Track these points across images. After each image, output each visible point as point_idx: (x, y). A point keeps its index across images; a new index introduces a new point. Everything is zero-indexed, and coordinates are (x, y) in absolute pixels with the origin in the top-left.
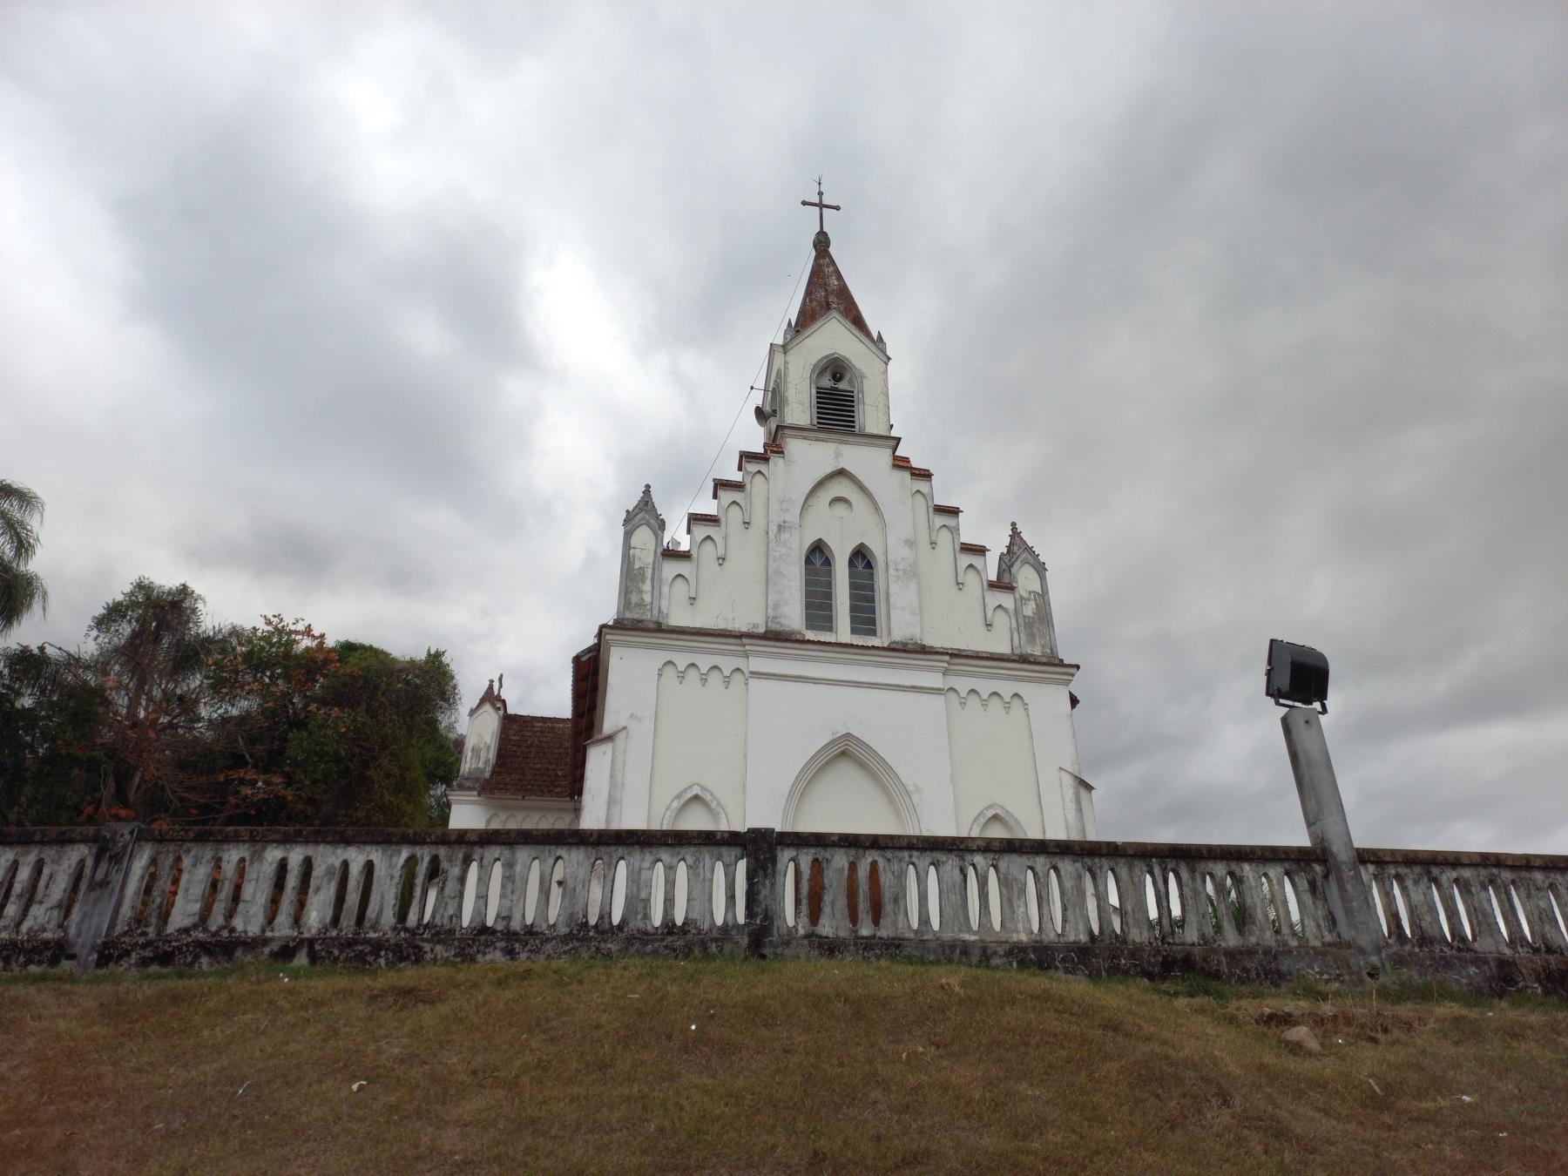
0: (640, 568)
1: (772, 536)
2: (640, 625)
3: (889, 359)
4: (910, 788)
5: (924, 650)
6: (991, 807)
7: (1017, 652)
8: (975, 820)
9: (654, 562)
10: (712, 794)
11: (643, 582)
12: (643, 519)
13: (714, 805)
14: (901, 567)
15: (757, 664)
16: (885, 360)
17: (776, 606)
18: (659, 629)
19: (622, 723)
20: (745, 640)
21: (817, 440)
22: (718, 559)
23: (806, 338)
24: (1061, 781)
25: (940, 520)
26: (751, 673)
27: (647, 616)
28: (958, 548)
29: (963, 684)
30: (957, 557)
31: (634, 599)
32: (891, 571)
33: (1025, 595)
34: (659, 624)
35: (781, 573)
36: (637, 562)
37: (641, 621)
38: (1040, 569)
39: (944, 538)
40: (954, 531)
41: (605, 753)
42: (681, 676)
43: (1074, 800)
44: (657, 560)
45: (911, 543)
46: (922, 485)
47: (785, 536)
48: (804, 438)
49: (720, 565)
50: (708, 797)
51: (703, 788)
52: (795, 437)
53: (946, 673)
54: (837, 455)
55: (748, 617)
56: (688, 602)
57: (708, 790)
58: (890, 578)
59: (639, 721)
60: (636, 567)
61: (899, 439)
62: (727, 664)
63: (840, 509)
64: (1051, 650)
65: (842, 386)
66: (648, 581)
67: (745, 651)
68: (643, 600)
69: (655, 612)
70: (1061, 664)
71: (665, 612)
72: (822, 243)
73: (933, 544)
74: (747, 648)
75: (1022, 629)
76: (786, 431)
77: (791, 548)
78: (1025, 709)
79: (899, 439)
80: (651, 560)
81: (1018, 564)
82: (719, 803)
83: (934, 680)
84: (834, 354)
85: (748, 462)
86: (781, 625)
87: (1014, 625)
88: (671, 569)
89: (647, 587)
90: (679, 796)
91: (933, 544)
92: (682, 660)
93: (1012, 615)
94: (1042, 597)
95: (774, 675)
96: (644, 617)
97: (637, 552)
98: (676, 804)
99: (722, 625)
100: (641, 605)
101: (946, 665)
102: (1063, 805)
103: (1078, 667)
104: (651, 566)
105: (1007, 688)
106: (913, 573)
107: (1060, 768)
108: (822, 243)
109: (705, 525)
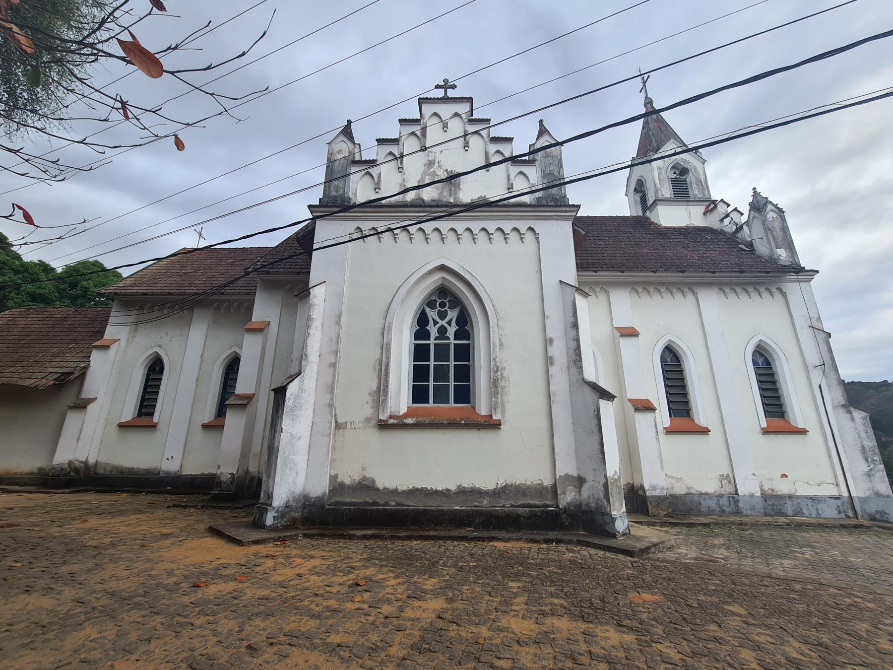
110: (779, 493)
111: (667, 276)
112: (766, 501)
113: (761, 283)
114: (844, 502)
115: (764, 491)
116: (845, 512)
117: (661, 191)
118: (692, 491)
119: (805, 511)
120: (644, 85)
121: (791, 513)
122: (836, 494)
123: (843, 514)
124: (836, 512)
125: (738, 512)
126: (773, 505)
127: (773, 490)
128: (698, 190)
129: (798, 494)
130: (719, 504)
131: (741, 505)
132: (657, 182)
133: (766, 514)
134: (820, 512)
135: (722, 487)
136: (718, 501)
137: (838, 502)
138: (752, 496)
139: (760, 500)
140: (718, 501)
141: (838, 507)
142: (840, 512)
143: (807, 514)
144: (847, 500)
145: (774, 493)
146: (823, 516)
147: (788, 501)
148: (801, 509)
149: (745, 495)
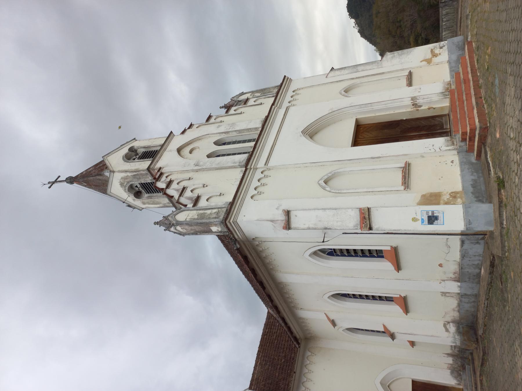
0: (198, 215)
1: (200, 168)
2: (228, 211)
3: (135, 139)
4: (330, 111)
5: (267, 117)
6: (341, 93)
7: (275, 95)
8: (346, 96)
9: (197, 210)
10: (325, 176)
11: (206, 213)
12: (172, 217)
13: (330, 175)
14: (229, 128)
15: (261, 164)
16: (135, 140)
17: (235, 163)
18: (232, 204)
19: (280, 212)
20: (249, 167)
21: (160, 158)
22: (204, 187)
23: (111, 165)
24: (332, 77)
25: (212, 120)
26: (265, 165)
27: (225, 210)
28: (226, 114)
29: (286, 104)
30: (229, 114)
31: (214, 216)
32: (230, 130)
33: (251, 96)
34: (230, 203)
35: (219, 163)
36: (194, 217)
37: (227, 210)
38: (243, 94)
39: (219, 119)
40: (218, 117)
41: (296, 216)
42: (260, 193)
43: (340, 71)
44: (196, 209)
45: (219, 127)
46: (195, 127)
47: (201, 163)
48: (157, 162)
49: (207, 186)
50: (326, 177)
51: (321, 179)
52: (155, 165)
53: (280, 108)
54: (171, 151)
55: (238, 174)
56: (222, 196)
57: (322, 178)
58: (233, 130)
59: (281, 205)
60: (197, 217)
61: (171, 132)
62: (258, 175)
63: (194, 152)
64: (276, 87)
65: (140, 155)
66: (206, 211)
67: (254, 169)
68: (215, 213)
69: (223, 206)
70: (282, 84)
71: (224, 203)
72: (71, 180)
73: (221, 122)
74: (252, 167)
75: (265, 94)
76: (151, 167)
77: (208, 161)
78: (300, 90)
79: (171, 132)
80: (195, 212)
81: (238, 99)
82: (329, 173)
83: (282, 112)
84: (123, 156)
85: (160, 181)
86: (244, 160)
87: (264, 97)
88: (202, 203)
89: (209, 212)
90: (324, 188)
91: (221, 122)
92: (252, 192)
93: (258, 98)
94: (253, 92)
95: (268, 157)
96: (225, 211)
97: (189, 217)
98: (328, 189)
99: (238, 183)
100: (217, 213)
101: (276, 108)
102: (342, 75)
103: (285, 76)
104: (198, 211)
105: (290, 93)
106: (233, 124)
107: (326, 77)
108: (71, 180)
109: (185, 192)
110: (458, 270)
111: (276, 296)
112: (465, 281)
113: (254, 249)
114: (466, 238)
115: (456, 278)
116: (478, 239)
117: (165, 204)
118: (457, 309)
119: (476, 263)
120: (53, 183)
121: (477, 271)
122: (458, 243)
123: (479, 241)
124: (477, 245)
125: (477, 296)
126: (469, 278)
127: (455, 273)
128: (145, 178)
129: (458, 260)
130: (468, 303)
131: (469, 293)
132: (158, 206)
133: (479, 282)
134: (477, 254)
135: (453, 297)
136: (465, 302)
137: (467, 242)
138: (460, 287)
139: (464, 284)
140: (465, 302)
141: (472, 243)
142: (478, 243)
143: (480, 262)
144: (463, 237)
145: (458, 273)
146: (482, 253)
147: (467, 270)
148: (474, 265)
149: (460, 290)
